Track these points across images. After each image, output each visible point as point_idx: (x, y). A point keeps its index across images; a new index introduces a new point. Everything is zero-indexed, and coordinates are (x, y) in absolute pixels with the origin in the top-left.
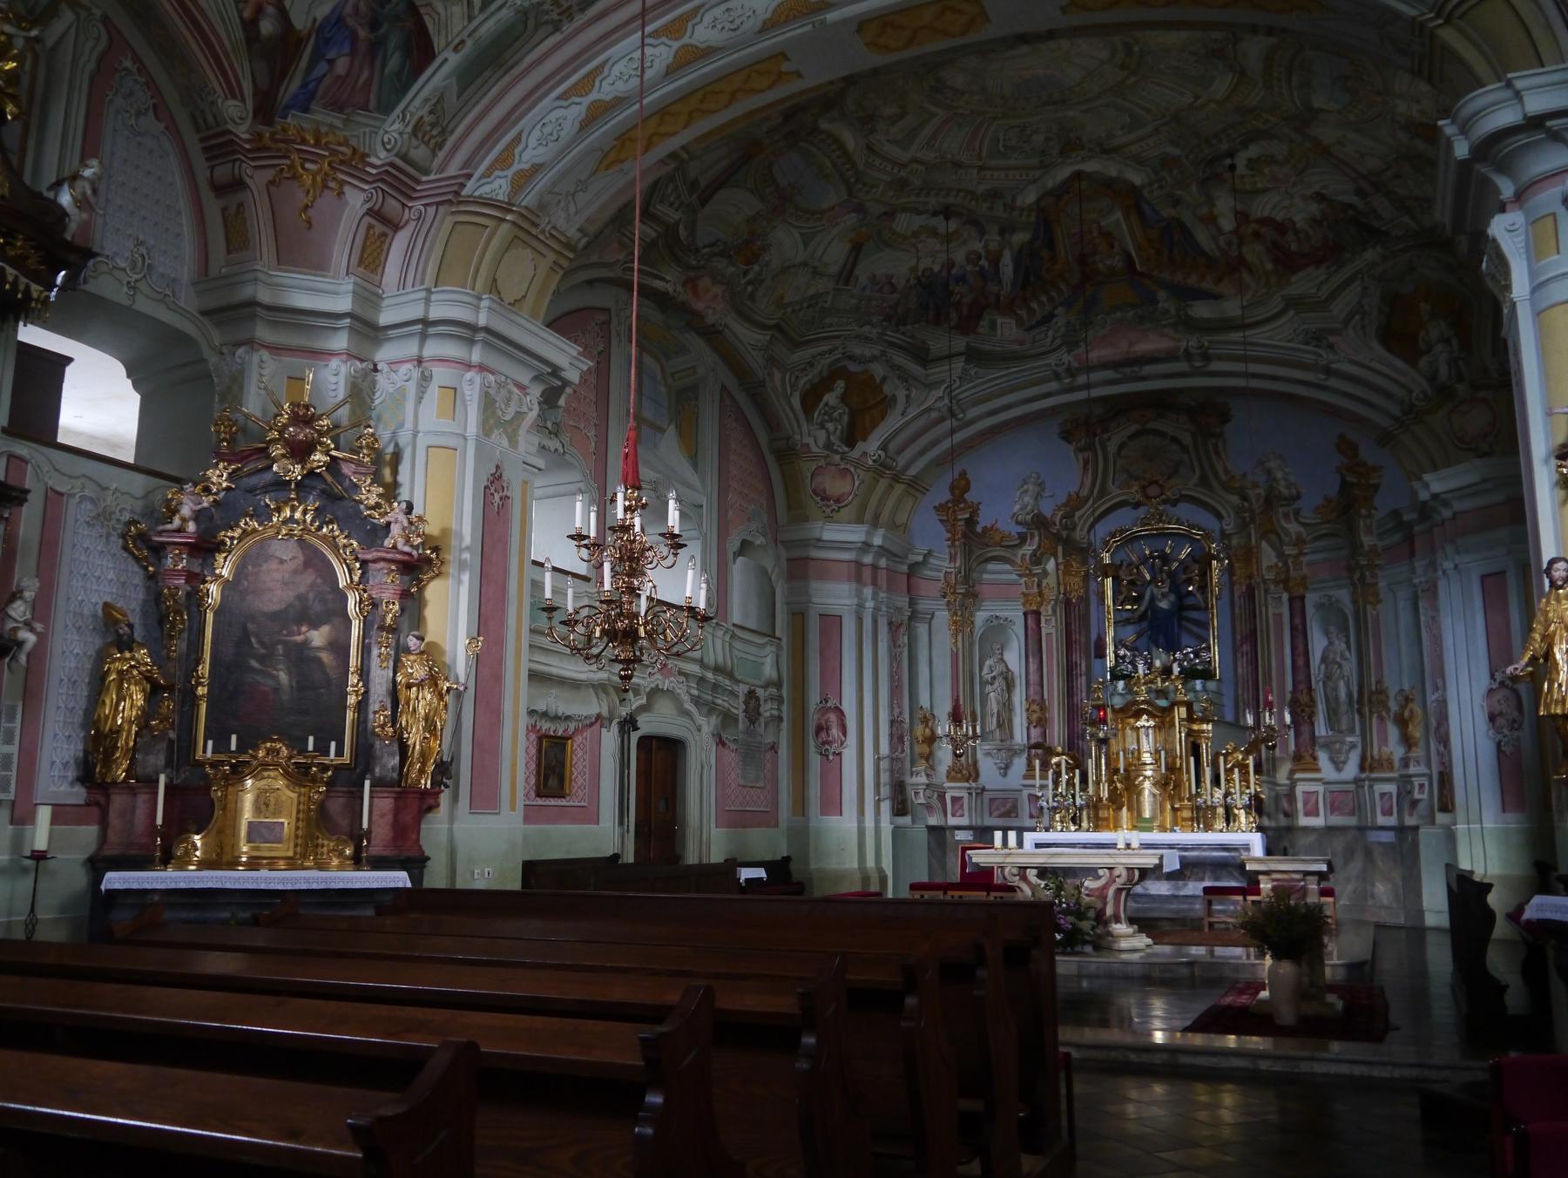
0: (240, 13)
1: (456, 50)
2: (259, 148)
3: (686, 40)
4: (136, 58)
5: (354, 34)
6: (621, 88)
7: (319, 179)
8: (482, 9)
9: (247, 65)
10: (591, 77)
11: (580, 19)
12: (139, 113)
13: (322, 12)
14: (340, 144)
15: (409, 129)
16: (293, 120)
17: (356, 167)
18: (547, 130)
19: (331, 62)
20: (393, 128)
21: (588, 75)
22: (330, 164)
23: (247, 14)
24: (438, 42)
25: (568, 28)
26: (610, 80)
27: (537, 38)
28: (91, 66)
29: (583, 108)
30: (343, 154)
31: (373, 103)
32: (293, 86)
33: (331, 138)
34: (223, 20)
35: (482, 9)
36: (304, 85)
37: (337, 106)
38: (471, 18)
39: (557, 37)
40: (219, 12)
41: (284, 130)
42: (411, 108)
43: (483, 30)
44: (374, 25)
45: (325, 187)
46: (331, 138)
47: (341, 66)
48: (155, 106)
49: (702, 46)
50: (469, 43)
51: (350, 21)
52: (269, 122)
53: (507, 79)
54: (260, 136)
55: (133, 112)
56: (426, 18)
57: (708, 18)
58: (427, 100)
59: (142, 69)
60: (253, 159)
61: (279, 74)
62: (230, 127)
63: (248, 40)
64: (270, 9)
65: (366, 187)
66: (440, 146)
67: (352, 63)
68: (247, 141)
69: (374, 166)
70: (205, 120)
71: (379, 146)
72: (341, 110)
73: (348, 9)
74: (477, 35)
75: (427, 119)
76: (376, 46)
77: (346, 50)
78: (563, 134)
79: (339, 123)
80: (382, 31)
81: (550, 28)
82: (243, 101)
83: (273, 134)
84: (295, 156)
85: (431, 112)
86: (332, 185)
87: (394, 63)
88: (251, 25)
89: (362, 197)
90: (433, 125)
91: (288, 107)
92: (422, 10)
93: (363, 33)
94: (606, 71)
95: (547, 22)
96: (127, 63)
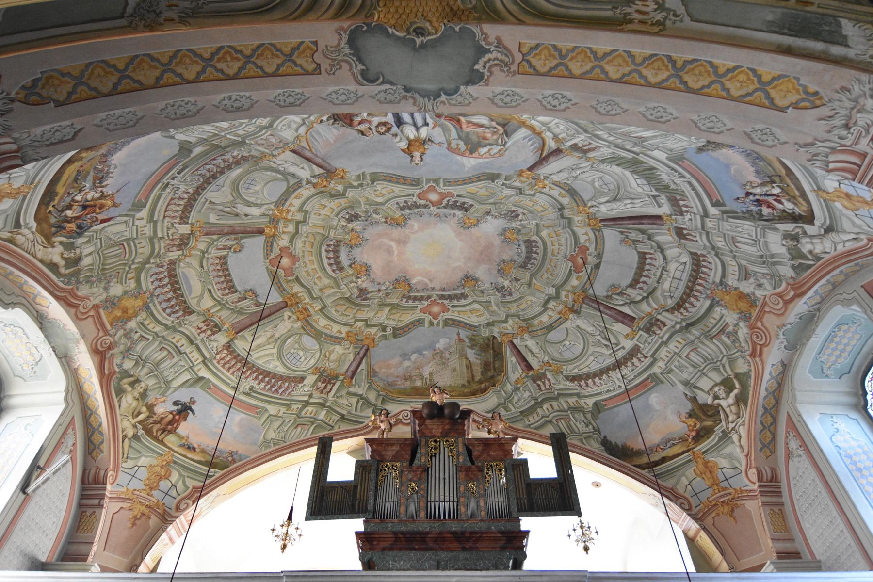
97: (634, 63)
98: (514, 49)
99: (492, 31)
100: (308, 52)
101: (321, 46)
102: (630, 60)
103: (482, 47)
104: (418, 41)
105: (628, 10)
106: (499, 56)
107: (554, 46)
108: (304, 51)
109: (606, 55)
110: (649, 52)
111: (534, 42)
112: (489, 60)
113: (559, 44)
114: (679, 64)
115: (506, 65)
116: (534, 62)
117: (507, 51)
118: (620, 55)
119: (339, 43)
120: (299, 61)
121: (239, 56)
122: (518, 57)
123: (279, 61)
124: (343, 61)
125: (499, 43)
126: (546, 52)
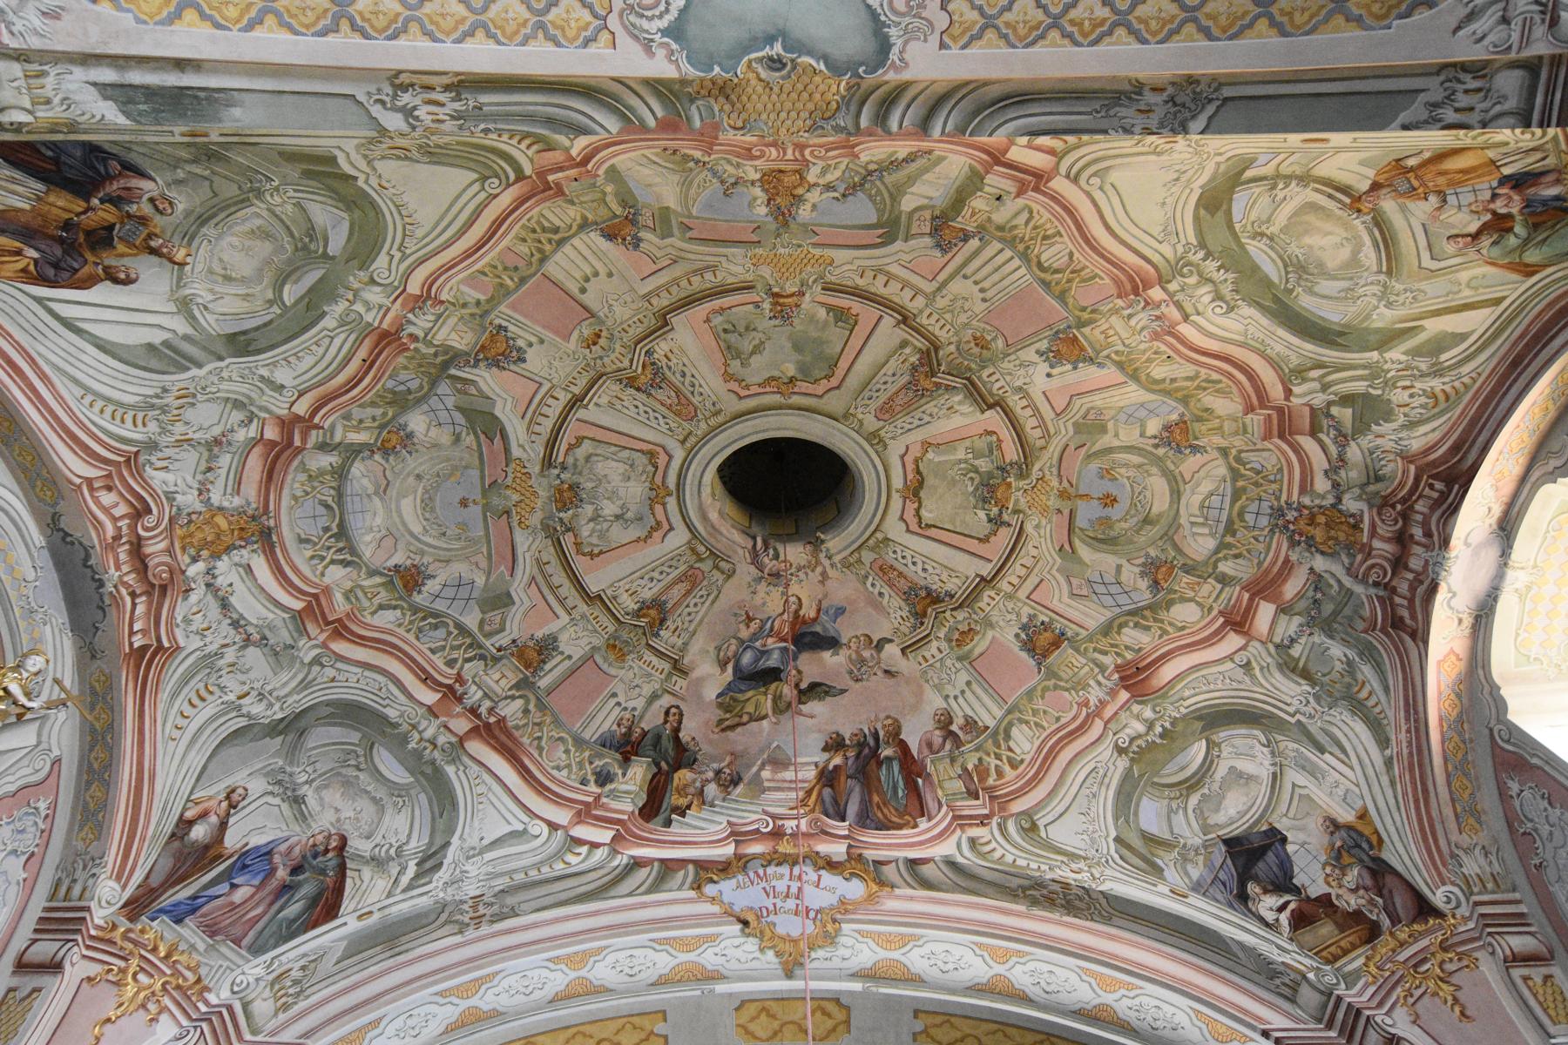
0: (185, 809)
1: (360, 917)
2: (104, 940)
3: (583, 973)
4: (54, 806)
5: (272, 871)
6: (504, 1002)
7: (142, 995)
8: (404, 891)
9: (153, 857)
10: (479, 982)
11: (485, 929)
12: (14, 852)
13: (257, 840)
14: (188, 968)
15: (271, 977)
16: (158, 929)
17: (189, 998)
18: (410, 1022)
19: (234, 886)
20: (254, 970)
21: (476, 980)
22: (164, 985)
23: (189, 815)
24: (347, 905)
25: (471, 934)
26: (496, 990)
27: (439, 933)
28: (13, 788)
29: (460, 1009)
30: (185, 979)
31: (245, 942)
32: (183, 893)
33: (183, 958)
34: (164, 809)
35: (404, 891)
36: (194, 897)
37: (212, 930)
38: (388, 897)
39: (458, 939)
40: (166, 802)
41: (142, 931)
42: (283, 958)
43: (394, 909)
44: (296, 870)
45: (143, 1006)
46: (183, 958)
47: (239, 896)
48: (33, 854)
49: (596, 983)
50: (376, 916)
51: (277, 859)
52: (132, 918)
53: (391, 962)
54: (114, 927)
55: (9, 848)
56: (349, 882)
57: (611, 959)
58: (305, 955)
59: (50, 818)
60: (88, 947)
61: (176, 878)
62: (93, 905)
63: (173, 835)
64: (213, 819)
65: (185, 1023)
66: (286, 1007)
67: (252, 896)
68: (98, 927)
69: (207, 1003)
70: (69, 889)
71: (227, 985)
72: (212, 935)
73: (283, 847)
74: (387, 911)
75: (295, 974)
76: (286, 889)
77: (256, 882)
78: (425, 1031)
79: (201, 946)
80: (301, 877)
81: (456, 928)
82: (124, 887)
83: (129, 930)
84: (134, 962)
85: (303, 968)
86: (152, 1007)
87: (294, 909)
88: (185, 824)
89: (175, 1031)
90: (296, 982)
91: (163, 911)
92: (349, 873)
93: (282, 873)
94: (496, 982)
95: (457, 922)
96: (42, 805)
97: (419, 21)
98: (622, 38)
99: (661, 67)
100: (956, 30)
101: (934, 39)
102: (430, 27)
103: (676, 40)
104: (777, 49)
105: (457, 105)
106: (645, 24)
107: (558, 44)
108: (964, 33)
109: (470, 33)
110: (401, 42)
111: (592, 49)
112: (661, 16)
113: (551, 47)
114: (345, 26)
115: (632, 7)
116: (586, 16)
117: (634, 33)
118: (448, 34)
119: (906, 43)
120: (975, 15)
121: (1069, 29)
122: (613, 22)
123: (1008, 16)
124: (903, 15)
125: (647, 46)
126: (571, 33)
